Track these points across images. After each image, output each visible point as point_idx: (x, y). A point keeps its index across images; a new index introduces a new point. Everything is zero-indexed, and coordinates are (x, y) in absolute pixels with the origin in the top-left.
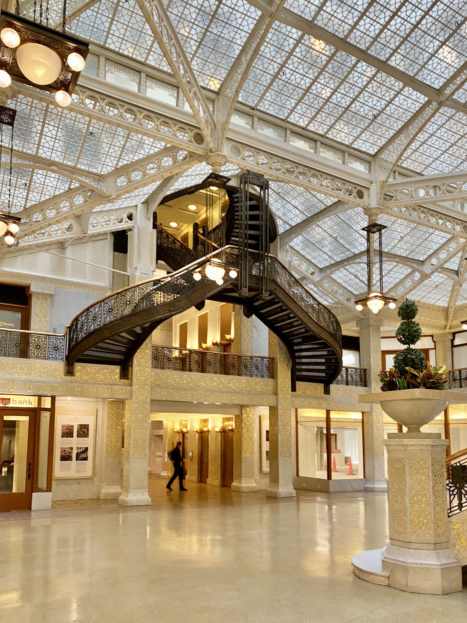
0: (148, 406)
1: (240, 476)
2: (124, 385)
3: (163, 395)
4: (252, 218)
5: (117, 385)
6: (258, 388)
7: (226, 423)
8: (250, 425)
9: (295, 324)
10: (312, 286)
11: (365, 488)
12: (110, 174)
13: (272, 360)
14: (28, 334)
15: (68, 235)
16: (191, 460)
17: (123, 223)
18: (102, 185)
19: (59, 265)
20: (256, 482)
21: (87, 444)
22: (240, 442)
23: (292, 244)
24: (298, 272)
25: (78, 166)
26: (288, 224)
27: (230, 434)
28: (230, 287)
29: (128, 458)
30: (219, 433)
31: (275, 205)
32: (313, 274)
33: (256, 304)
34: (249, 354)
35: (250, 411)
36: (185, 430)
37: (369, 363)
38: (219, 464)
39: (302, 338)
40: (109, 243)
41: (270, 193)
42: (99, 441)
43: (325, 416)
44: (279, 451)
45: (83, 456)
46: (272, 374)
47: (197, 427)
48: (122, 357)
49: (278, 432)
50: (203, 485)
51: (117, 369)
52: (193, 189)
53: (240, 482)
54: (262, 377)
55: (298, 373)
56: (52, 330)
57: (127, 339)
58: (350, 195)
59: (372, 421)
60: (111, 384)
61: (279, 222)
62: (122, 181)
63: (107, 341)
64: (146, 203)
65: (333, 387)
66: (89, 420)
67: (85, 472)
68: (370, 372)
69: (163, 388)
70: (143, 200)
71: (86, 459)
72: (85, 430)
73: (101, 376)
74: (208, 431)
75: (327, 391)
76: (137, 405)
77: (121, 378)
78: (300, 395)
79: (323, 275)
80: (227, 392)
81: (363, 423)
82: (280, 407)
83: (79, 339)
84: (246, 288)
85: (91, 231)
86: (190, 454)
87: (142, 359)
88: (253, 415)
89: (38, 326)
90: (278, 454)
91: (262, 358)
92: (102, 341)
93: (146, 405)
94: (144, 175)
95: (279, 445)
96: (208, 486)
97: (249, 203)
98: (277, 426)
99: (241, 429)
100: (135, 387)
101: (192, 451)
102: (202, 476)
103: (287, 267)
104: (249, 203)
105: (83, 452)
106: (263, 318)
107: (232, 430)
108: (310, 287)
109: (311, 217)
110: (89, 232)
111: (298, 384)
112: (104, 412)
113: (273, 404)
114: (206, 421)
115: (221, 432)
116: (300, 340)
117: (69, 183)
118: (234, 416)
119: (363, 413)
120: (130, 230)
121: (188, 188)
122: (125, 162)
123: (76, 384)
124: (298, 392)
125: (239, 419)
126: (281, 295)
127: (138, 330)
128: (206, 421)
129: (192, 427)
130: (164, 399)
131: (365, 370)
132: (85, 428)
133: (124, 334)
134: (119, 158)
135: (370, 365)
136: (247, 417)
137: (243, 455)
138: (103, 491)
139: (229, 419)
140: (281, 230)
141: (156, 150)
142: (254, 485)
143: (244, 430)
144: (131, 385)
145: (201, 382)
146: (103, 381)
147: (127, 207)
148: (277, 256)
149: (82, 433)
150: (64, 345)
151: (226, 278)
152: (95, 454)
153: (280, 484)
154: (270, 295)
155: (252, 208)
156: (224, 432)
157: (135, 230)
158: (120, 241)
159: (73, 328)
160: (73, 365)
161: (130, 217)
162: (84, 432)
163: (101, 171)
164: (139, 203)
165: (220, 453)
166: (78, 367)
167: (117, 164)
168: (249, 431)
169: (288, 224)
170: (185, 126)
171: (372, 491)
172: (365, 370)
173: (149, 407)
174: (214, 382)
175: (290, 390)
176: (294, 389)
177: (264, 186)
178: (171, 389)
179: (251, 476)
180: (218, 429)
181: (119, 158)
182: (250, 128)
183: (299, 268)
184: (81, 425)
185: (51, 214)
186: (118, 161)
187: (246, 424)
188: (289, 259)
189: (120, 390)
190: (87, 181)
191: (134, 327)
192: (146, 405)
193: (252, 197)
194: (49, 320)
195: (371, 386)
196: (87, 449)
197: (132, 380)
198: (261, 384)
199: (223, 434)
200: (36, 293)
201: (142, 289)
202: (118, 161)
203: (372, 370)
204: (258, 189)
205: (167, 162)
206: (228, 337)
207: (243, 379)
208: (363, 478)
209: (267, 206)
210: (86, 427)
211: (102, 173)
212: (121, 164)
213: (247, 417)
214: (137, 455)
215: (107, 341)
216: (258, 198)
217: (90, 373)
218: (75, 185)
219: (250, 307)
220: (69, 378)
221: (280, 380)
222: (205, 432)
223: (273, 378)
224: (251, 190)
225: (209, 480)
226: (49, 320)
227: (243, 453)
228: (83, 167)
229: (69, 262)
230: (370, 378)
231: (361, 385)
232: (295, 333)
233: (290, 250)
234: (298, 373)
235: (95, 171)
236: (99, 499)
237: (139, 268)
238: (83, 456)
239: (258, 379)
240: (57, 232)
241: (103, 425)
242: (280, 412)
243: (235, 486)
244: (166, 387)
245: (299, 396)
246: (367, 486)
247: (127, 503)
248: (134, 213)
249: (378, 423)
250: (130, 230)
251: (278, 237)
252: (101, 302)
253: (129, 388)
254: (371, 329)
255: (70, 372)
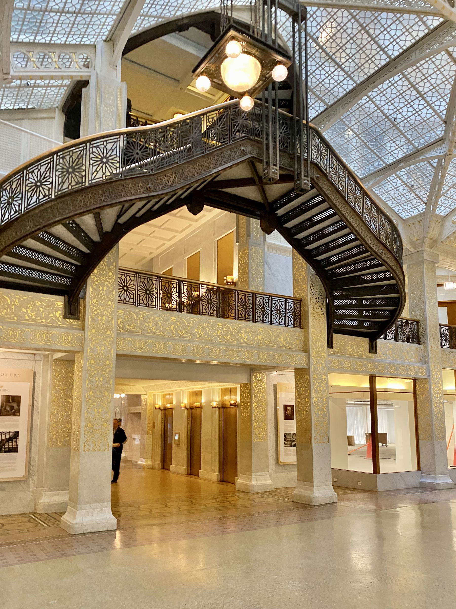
0: (112, 363)
1: (249, 470)
3: (137, 346)
5: (59, 327)
6: (282, 341)
7: (227, 398)
8: (263, 397)
11: (421, 483)
16: (178, 445)
20: (271, 477)
21: (17, 426)
22: (249, 421)
27: (233, 410)
29: (77, 450)
30: (217, 409)
35: (263, 377)
36: (169, 406)
37: (423, 311)
38: (217, 451)
42: (37, 421)
43: (367, 385)
44: (313, 436)
45: (11, 445)
47: (185, 401)
48: (68, 282)
49: (310, 406)
50: (193, 479)
51: (59, 302)
53: (250, 480)
54: (286, 325)
55: (337, 322)
57: (77, 249)
59: (430, 391)
60: (47, 326)
65: (380, 342)
66: (21, 389)
67: (14, 470)
68: (425, 324)
69: (138, 335)
71: (15, 450)
72: (15, 405)
73: (29, 311)
74: (201, 407)
75: (373, 349)
76: (92, 362)
77: (65, 317)
78: (338, 353)
80: (237, 345)
81: (415, 393)
82: (312, 369)
84: (276, 165)
86: (177, 438)
87: (101, 287)
88: (266, 384)
90: (310, 439)
93: (108, 362)
95: (313, 426)
96: (200, 481)
98: (310, 398)
99: (251, 403)
100: (89, 332)
101: (179, 434)
102: (193, 465)
105: (10, 439)
107: (235, 405)
112: (46, 377)
113: (302, 365)
114: (197, 394)
115: (219, 408)
118: (238, 387)
119: (414, 380)
124: (335, 349)
125: (247, 389)
128: (197, 394)
129: (179, 402)
130: (139, 353)
131: (418, 322)
132: (13, 401)
135: (425, 314)
136: (259, 386)
137: (254, 440)
138: (42, 501)
139: (230, 391)
142: (270, 482)
143: (255, 405)
144: (83, 329)
145: (198, 329)
146: (33, 320)
149: (8, 409)
152: (30, 442)
153: (315, 484)
156: (222, 407)
157: (92, 82)
162: (12, 408)
165: (217, 436)
168: (261, 406)
171: (433, 488)
172: (418, 322)
173: (113, 365)
174: (217, 329)
175: (326, 345)
176: (330, 345)
178: (152, 338)
179: (264, 469)
180: (214, 404)
184: (8, 397)
187: (256, 397)
189: (64, 334)
191: (81, 214)
192: (108, 362)
195: (426, 343)
196: (16, 435)
197: (84, 320)
198: (284, 335)
199: (221, 410)
201: (97, 147)
203: (428, 321)
207: (260, 327)
208: (416, 469)
210: (16, 399)
213: (259, 386)
214: (92, 445)
217: (9, 306)
221: (312, 331)
222: (196, 408)
223: (300, 327)
225: (202, 472)
227: (253, 438)
230: (425, 332)
231: (413, 342)
234: (337, 322)
236: (34, 513)
238: (11, 445)
239: (282, 328)
241: (44, 397)
242: (313, 377)
243: (241, 484)
244: (143, 335)
245: (336, 354)
246: (424, 480)
247: (73, 528)
248: (91, 56)
249: (438, 393)
252: (21, 170)
254: (425, 266)
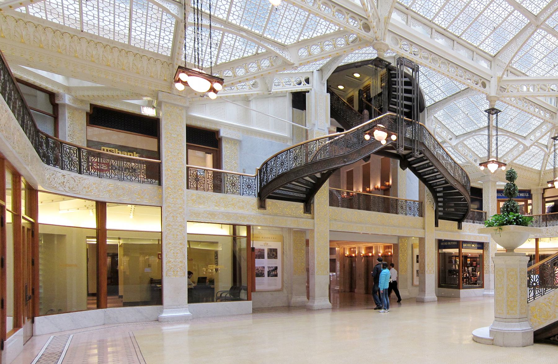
2: (307, 218)
4: (407, 91)
9: (438, 177)
10: (450, 149)
12: (293, 46)
13: (421, 204)
14: (220, 172)
15: (255, 91)
17: (302, 85)
18: (286, 53)
19: (246, 117)
23: (436, 115)
24: (441, 137)
25: (265, 35)
26: (433, 100)
28: (390, 145)
31: (423, 84)
32: (451, 139)
33: (409, 160)
34: (404, 198)
39: (444, 187)
40: (288, 102)
41: (420, 74)
46: (421, 214)
52: (360, 64)
56: (242, 170)
58: (476, 84)
61: (426, 98)
62: (303, 53)
63: (294, 183)
64: (321, 70)
70: (318, 68)
79: (458, 141)
83: (270, 180)
85: (274, 89)
89: (229, 166)
91: (414, 202)
92: (290, 183)
94: (322, 51)
97: (404, 80)
103: (432, 133)
104: (404, 80)
106: (415, 171)
108: (449, 150)
109: (450, 97)
110: (273, 91)
111: (440, 221)
116: (442, 189)
117: (256, 48)
120: (308, 92)
121: (355, 63)
122: (306, 38)
123: (268, 216)
126: (428, 154)
127: (318, 175)
133: (307, 178)
134: (301, 33)
140: (427, 104)
141: (332, 31)
147: (305, 72)
148: (425, 124)
150: (256, 185)
151: (388, 138)
154: (420, 154)
155: (407, 84)
158: (299, 100)
159: (263, 171)
160: (264, 201)
161: (307, 81)
163: (285, 42)
164: (315, 71)
166: (269, 202)
167: (299, 38)
169: (433, 100)
170: (355, 16)
177: (416, 69)
181: (301, 33)
182: (405, 23)
183: (440, 135)
185: (241, 72)
186: (300, 36)
188: (434, 126)
190: (272, 48)
193: (406, 76)
194: (242, 162)
200: (230, 140)
202: (300, 36)
204: (411, 70)
205: (341, 42)
206: (387, 183)
209: (418, 85)
211: (286, 44)
212: (302, 38)
215: (294, 183)
216: (411, 77)
218: (261, 51)
219: (405, 163)
220: (262, 211)
224: (405, 70)
226: (242, 162)
228: (269, 37)
229: (253, 114)
232: (438, 183)
233: (434, 120)
235: (279, 41)
237: (316, 125)
240: (244, 89)
250: (308, 92)
251: (426, 109)
253: (312, 220)
255: (262, 206)
